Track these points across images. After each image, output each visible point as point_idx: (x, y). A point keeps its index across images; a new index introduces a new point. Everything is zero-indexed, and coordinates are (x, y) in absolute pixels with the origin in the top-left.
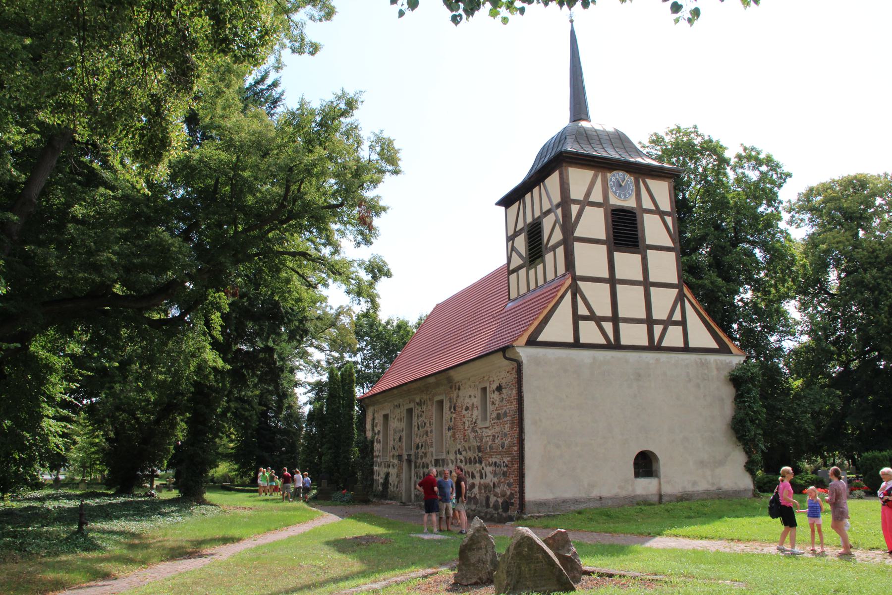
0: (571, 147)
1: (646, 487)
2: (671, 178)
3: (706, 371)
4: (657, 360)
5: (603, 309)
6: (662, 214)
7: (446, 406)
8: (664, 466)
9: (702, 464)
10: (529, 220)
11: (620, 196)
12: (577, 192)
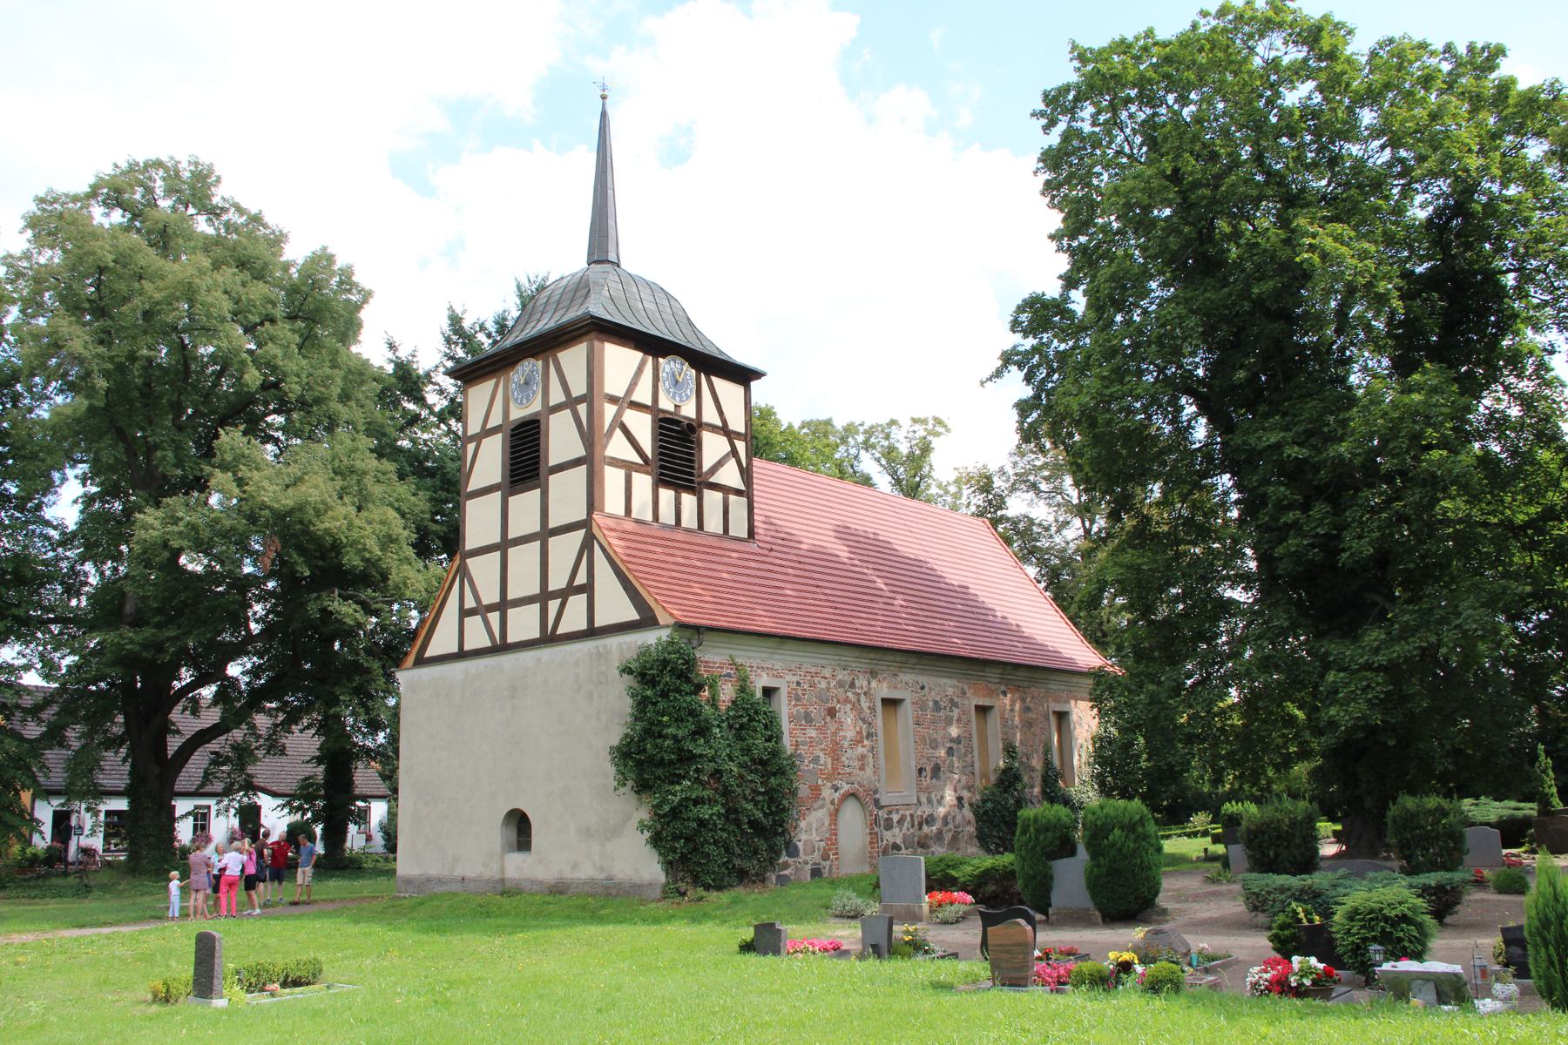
1: (518, 866)
3: (604, 668)
4: (539, 660)
9: (587, 832)
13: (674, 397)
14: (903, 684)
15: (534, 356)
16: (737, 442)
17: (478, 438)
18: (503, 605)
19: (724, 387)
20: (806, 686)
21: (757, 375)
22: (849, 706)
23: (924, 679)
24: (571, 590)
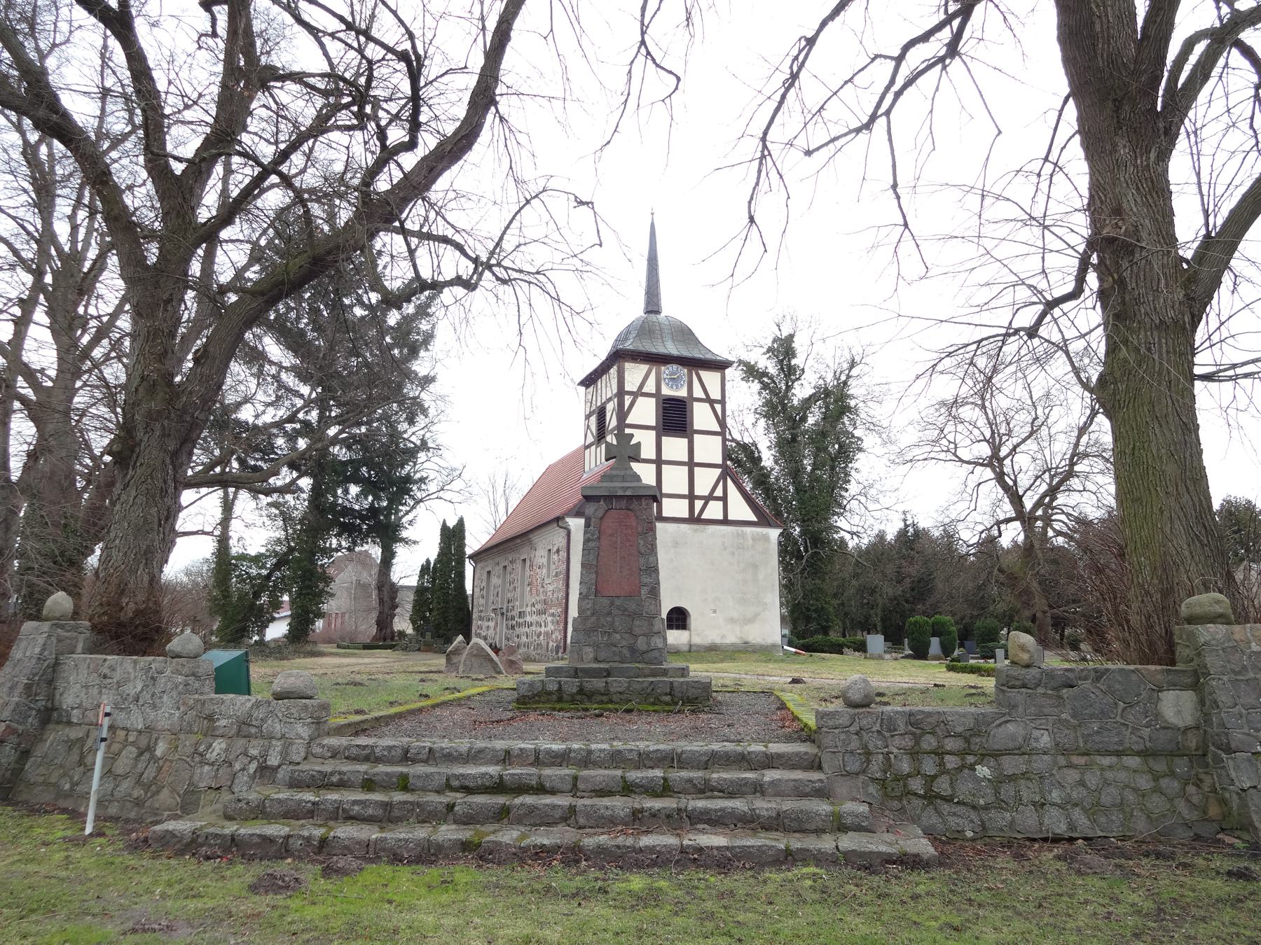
0: (629, 345)
6: (711, 402)
7: (528, 563)
8: (694, 621)
9: (732, 620)
10: (599, 404)
11: (672, 387)
12: (631, 385)
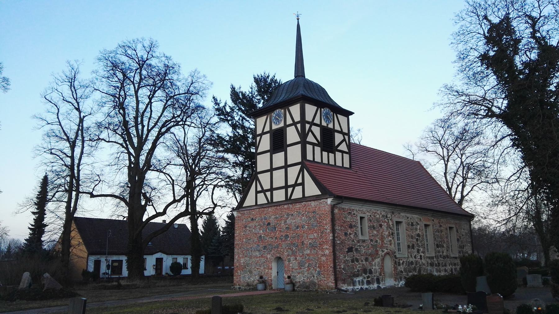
2: (300, 100)
5: (267, 186)
13: (326, 122)
14: (403, 217)
15: (281, 108)
16: (345, 136)
17: (261, 135)
18: (272, 190)
19: (342, 118)
20: (373, 217)
21: (352, 113)
22: (386, 224)
23: (408, 215)
24: (296, 185)
